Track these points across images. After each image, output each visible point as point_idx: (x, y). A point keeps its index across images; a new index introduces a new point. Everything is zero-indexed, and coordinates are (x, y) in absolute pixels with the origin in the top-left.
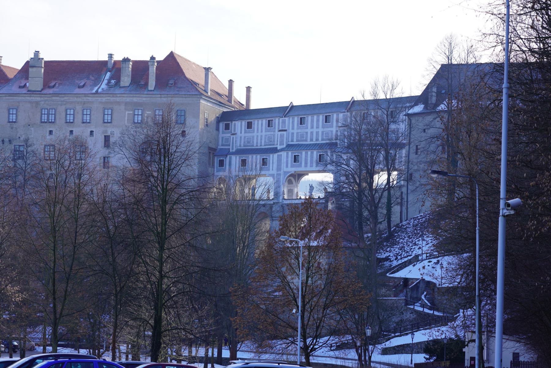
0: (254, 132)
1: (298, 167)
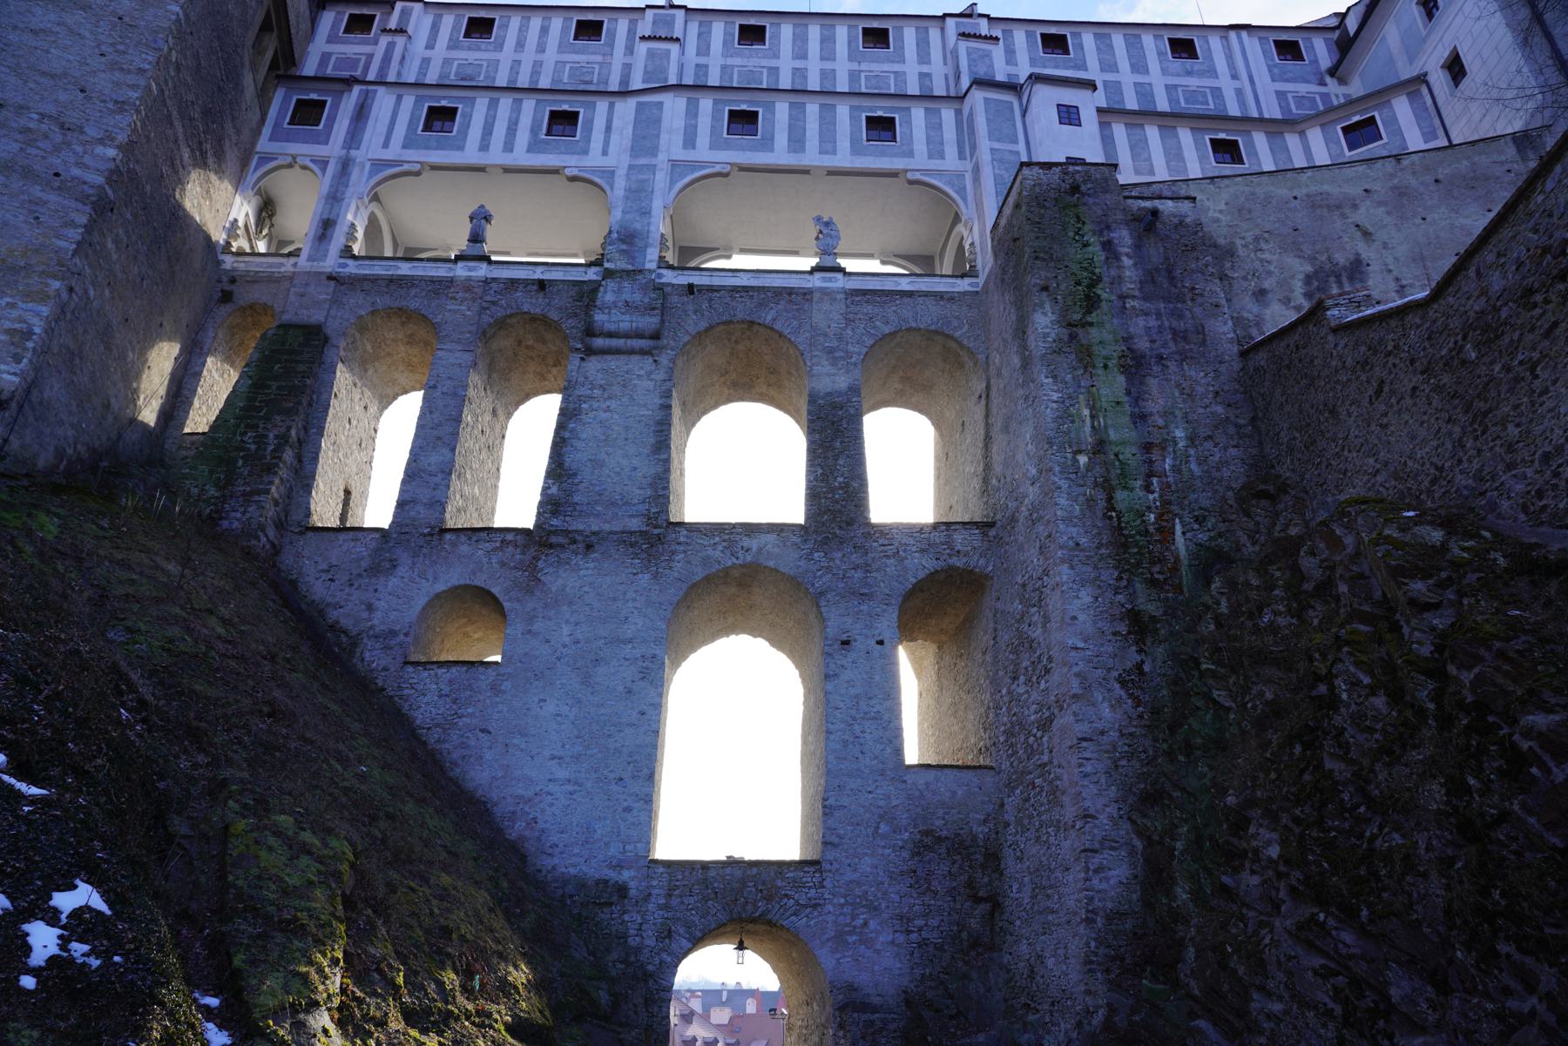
0: (499, 47)
1: (753, 149)
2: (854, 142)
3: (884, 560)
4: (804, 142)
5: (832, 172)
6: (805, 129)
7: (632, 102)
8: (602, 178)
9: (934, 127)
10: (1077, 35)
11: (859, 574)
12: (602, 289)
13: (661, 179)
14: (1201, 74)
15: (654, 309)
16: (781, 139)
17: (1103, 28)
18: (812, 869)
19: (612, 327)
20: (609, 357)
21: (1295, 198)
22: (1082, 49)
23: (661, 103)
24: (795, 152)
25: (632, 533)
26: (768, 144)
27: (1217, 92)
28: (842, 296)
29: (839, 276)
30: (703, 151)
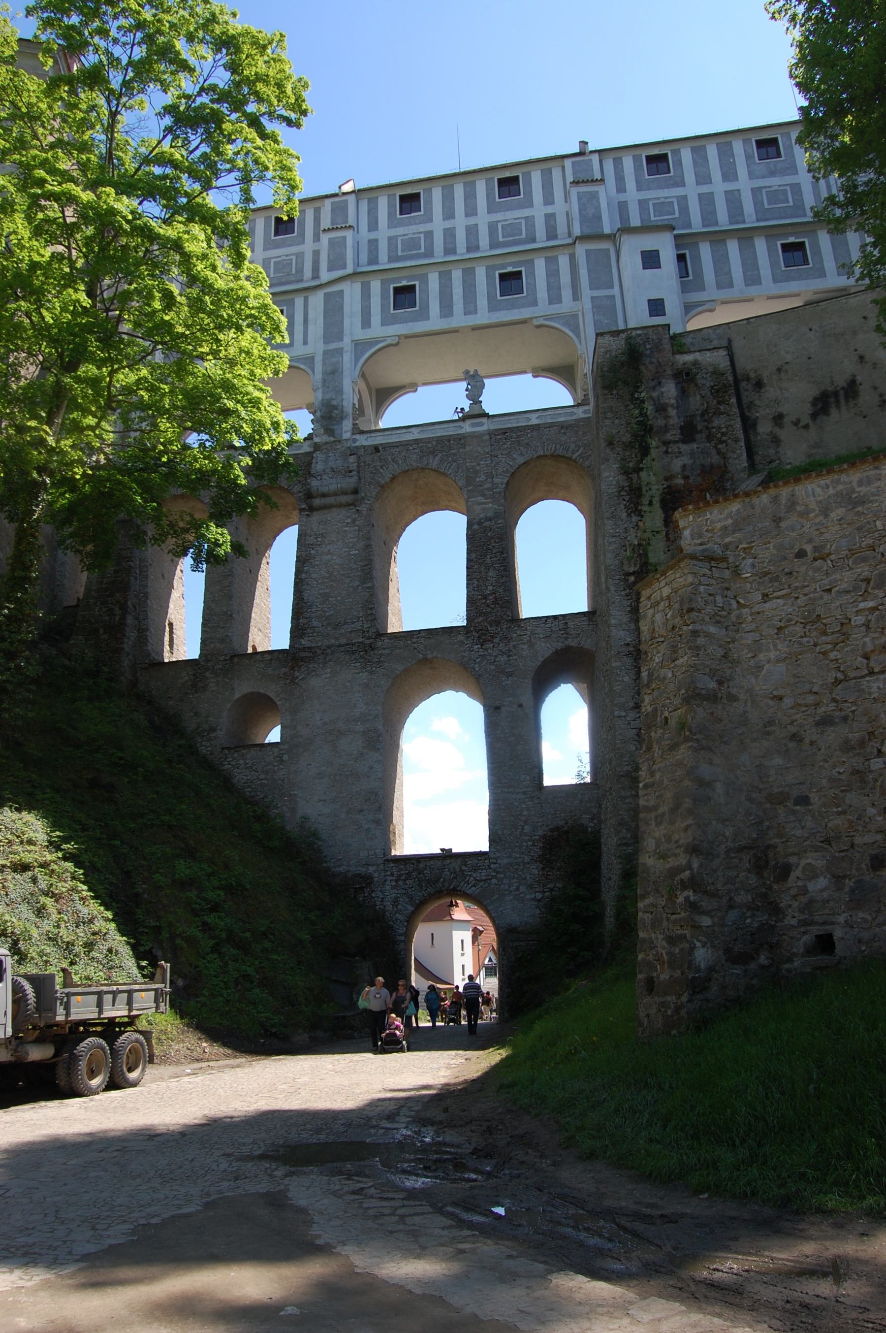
1: (414, 320)
2: (491, 297)
3: (522, 646)
4: (452, 307)
5: (475, 328)
6: (452, 295)
7: (319, 296)
8: (304, 364)
9: (553, 273)
10: (677, 152)
11: (504, 658)
12: (314, 461)
13: (347, 358)
14: (783, 172)
15: (351, 471)
16: (434, 307)
17: (697, 142)
18: (483, 858)
19: (325, 490)
20: (326, 511)
21: (811, 330)
22: (681, 164)
23: (342, 291)
24: (446, 317)
25: (353, 644)
26: (424, 315)
27: (796, 188)
28: (487, 437)
29: (484, 420)
30: (377, 330)
